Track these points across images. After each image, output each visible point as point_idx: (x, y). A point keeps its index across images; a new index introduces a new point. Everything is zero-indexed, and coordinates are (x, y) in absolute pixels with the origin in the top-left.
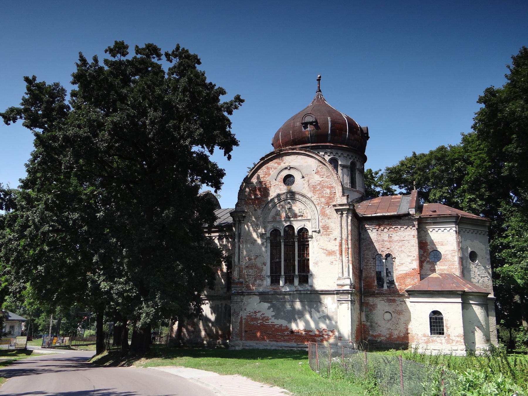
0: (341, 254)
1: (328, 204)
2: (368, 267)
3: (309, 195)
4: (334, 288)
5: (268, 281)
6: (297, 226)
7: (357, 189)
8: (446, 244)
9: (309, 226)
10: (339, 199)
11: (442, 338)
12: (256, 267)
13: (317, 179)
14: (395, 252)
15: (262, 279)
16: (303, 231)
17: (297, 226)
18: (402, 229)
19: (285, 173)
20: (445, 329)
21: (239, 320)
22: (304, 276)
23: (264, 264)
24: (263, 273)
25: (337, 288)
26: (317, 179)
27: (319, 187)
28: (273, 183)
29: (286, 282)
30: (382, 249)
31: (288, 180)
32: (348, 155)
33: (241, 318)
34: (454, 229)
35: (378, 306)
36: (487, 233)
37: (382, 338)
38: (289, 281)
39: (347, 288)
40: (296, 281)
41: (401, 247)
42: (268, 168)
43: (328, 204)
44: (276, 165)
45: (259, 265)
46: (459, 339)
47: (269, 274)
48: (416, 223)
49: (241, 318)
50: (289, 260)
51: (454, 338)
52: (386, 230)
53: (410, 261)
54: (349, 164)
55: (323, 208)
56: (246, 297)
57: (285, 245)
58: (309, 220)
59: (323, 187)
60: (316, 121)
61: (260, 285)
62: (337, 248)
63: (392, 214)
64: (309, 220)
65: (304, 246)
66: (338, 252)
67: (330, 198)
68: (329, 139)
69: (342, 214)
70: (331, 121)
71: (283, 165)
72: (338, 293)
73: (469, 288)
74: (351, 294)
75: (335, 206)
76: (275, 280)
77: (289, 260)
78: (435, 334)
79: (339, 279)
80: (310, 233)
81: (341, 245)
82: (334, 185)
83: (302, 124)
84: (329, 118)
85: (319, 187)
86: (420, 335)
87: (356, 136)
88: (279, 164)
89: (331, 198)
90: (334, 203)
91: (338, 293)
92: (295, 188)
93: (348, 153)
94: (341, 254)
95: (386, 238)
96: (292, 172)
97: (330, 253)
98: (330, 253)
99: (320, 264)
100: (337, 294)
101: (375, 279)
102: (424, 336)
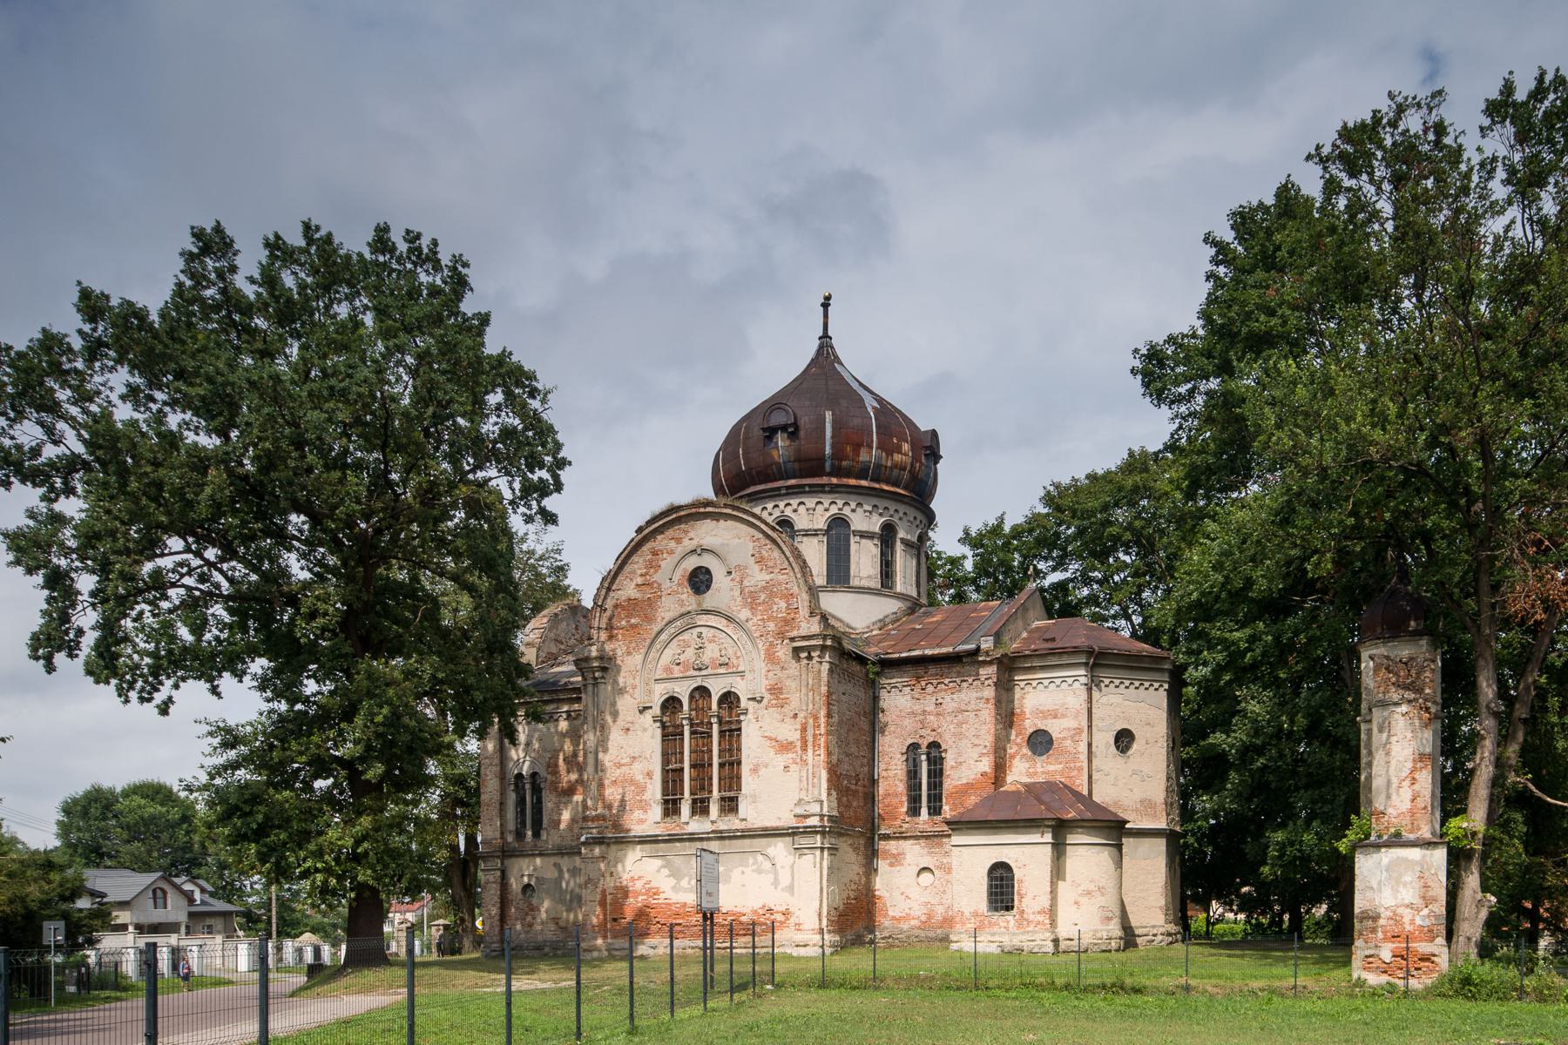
0: (804, 748)
1: (781, 635)
2: (891, 773)
3: (744, 614)
4: (787, 820)
5: (657, 811)
6: (717, 688)
7: (899, 588)
8: (1064, 716)
9: (742, 689)
10: (803, 625)
11: (1009, 919)
12: (632, 782)
13: (758, 577)
14: (947, 736)
15: (644, 806)
16: (729, 699)
17: (717, 688)
18: (965, 685)
19: (692, 563)
20: (1016, 898)
21: (598, 897)
22: (702, 801)
23: (649, 775)
24: (647, 796)
25: (793, 823)
26: (758, 577)
27: (763, 596)
28: (666, 585)
29: (693, 813)
30: (923, 732)
31: (700, 580)
32: (875, 506)
33: (604, 891)
34: (1083, 680)
35: (908, 857)
36: (1166, 686)
37: (913, 922)
38: (700, 808)
39: (814, 821)
40: (714, 809)
41: (960, 724)
42: (655, 553)
43: (781, 635)
44: (673, 544)
45: (640, 778)
46: (1040, 918)
47: (659, 796)
48: (990, 671)
49: (604, 891)
50: (701, 766)
51: (1031, 917)
52: (930, 688)
53: (976, 756)
54: (877, 529)
55: (772, 645)
56: (614, 848)
57: (692, 733)
58: (741, 674)
59: (772, 595)
60: (796, 425)
61: (642, 821)
62: (798, 735)
63: (944, 650)
64: (741, 674)
65: (732, 733)
66: (799, 744)
67: (786, 622)
68: (828, 469)
69: (810, 658)
70: (834, 422)
71: (688, 544)
72: (792, 833)
73: (1079, 812)
74: (823, 833)
75: (792, 639)
76: (671, 808)
77: (701, 766)
78: (996, 910)
79: (800, 802)
80: (744, 703)
81: (804, 729)
82: (795, 590)
83: (764, 430)
84: (828, 415)
85: (763, 596)
86: (967, 914)
87: (897, 457)
88: (679, 541)
89: (788, 622)
90: (795, 633)
91: (792, 833)
92: (710, 599)
93: (875, 501)
94: (804, 748)
95: (931, 708)
96: (707, 561)
97: (785, 747)
98: (785, 747)
99: (763, 771)
100: (794, 834)
101: (905, 799)
102: (976, 914)
